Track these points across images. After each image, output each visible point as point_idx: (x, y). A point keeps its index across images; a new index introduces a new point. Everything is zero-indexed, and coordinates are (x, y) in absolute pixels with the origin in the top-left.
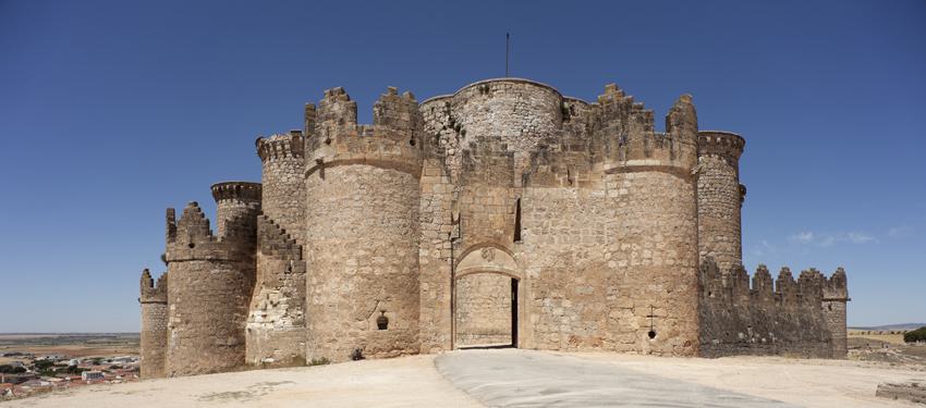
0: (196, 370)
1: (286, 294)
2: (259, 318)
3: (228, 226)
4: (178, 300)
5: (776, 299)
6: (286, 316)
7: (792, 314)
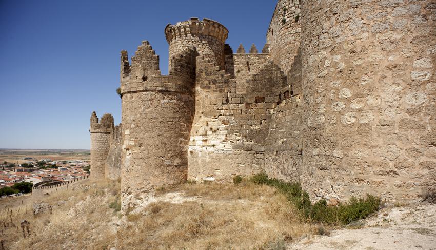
0: (148, 187)
1: (224, 122)
2: (200, 142)
3: (175, 63)
4: (133, 126)
6: (226, 140)
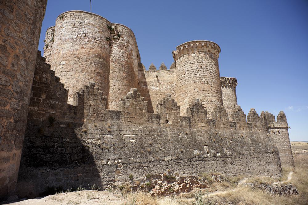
5: (231, 126)
7: (244, 136)
